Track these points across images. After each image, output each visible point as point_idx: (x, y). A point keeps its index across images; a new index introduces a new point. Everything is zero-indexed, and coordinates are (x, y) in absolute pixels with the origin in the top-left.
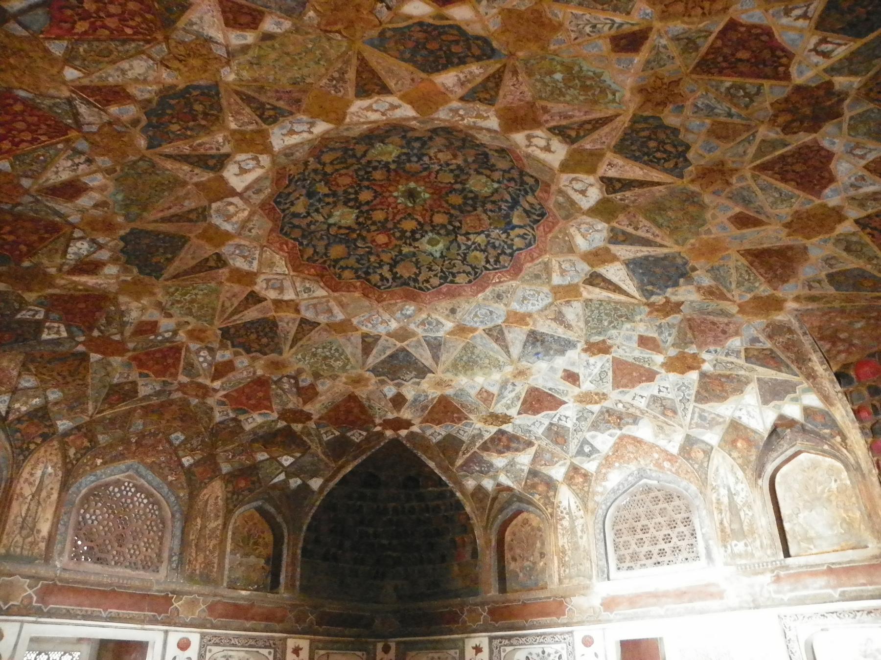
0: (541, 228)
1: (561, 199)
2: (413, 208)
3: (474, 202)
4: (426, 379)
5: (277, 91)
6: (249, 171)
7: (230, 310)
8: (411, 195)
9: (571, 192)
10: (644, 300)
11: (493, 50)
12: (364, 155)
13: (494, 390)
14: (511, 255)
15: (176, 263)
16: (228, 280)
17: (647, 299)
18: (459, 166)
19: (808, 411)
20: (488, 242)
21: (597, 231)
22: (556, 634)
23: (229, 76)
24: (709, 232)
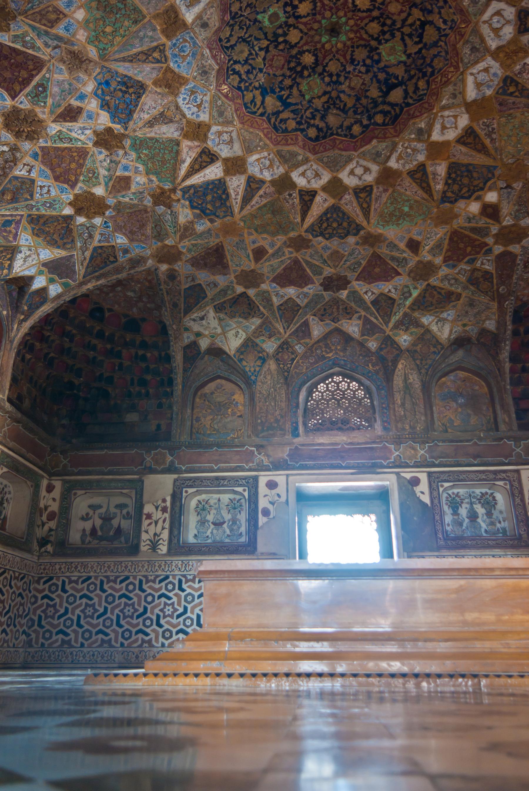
0: (265, 126)
1: (300, 158)
2: (319, 22)
5: (518, 108)
6: (493, 15)
8: (334, 31)
9: (305, 167)
10: (180, 187)
11: (445, 202)
12: (403, 39)
13: (60, 30)
14: (239, 88)
17: (181, 190)
18: (341, 84)
19: (44, 290)
20: (253, 68)
21: (261, 170)
24: (250, 234)
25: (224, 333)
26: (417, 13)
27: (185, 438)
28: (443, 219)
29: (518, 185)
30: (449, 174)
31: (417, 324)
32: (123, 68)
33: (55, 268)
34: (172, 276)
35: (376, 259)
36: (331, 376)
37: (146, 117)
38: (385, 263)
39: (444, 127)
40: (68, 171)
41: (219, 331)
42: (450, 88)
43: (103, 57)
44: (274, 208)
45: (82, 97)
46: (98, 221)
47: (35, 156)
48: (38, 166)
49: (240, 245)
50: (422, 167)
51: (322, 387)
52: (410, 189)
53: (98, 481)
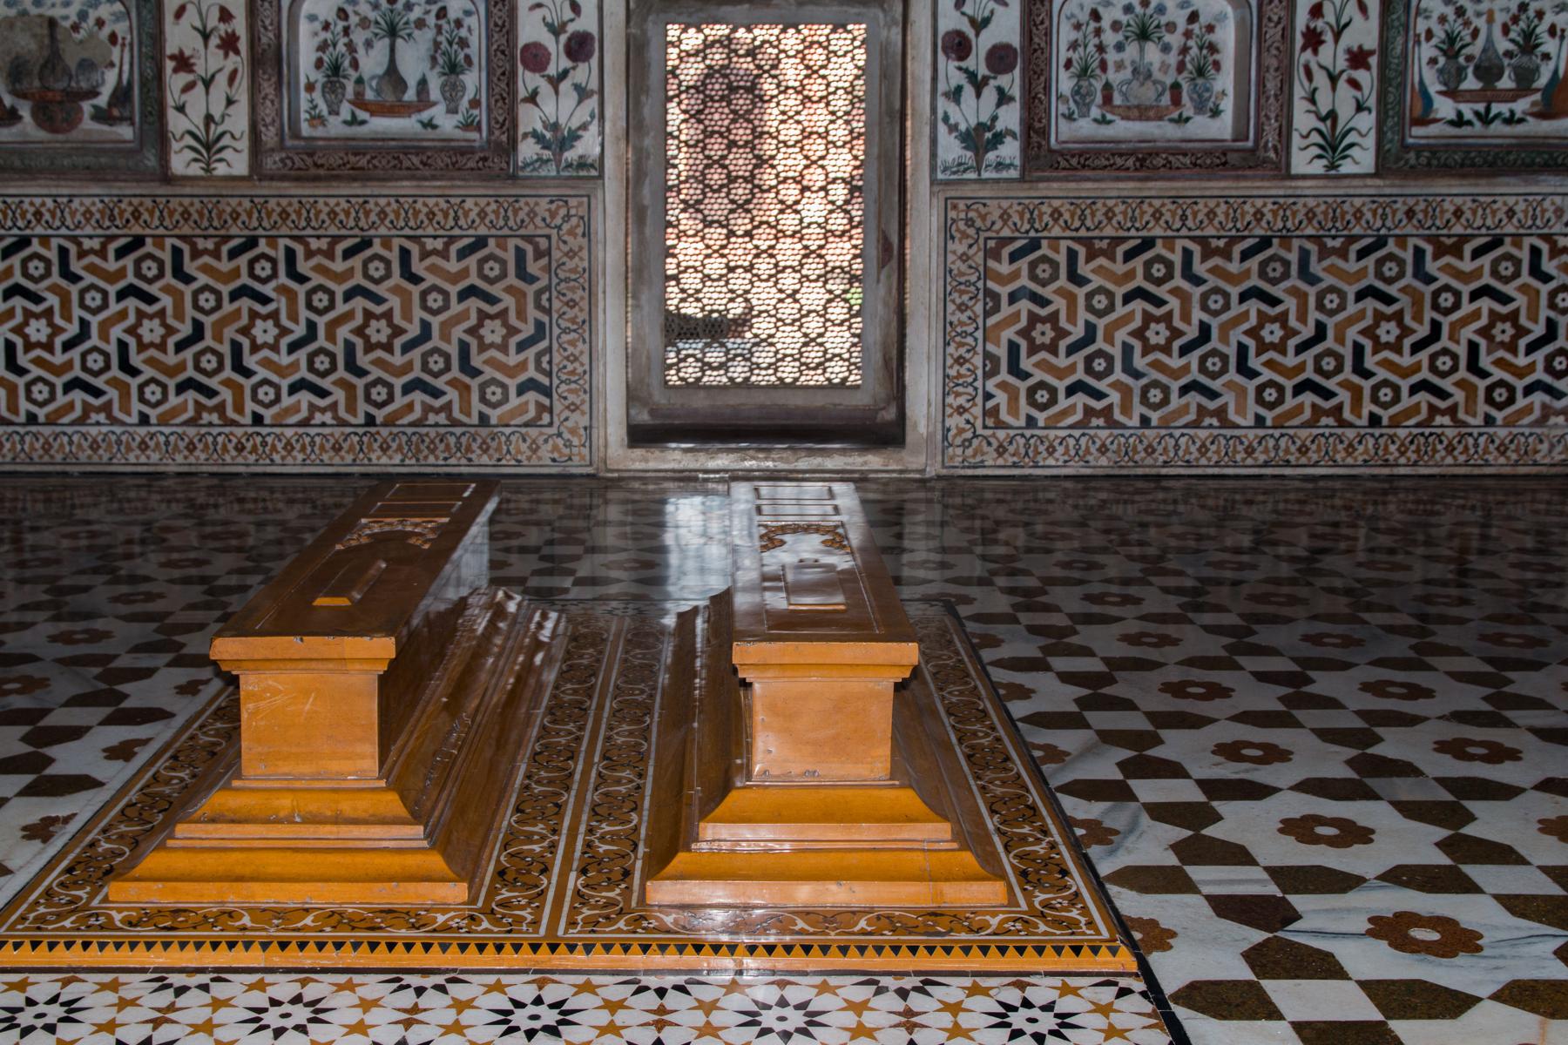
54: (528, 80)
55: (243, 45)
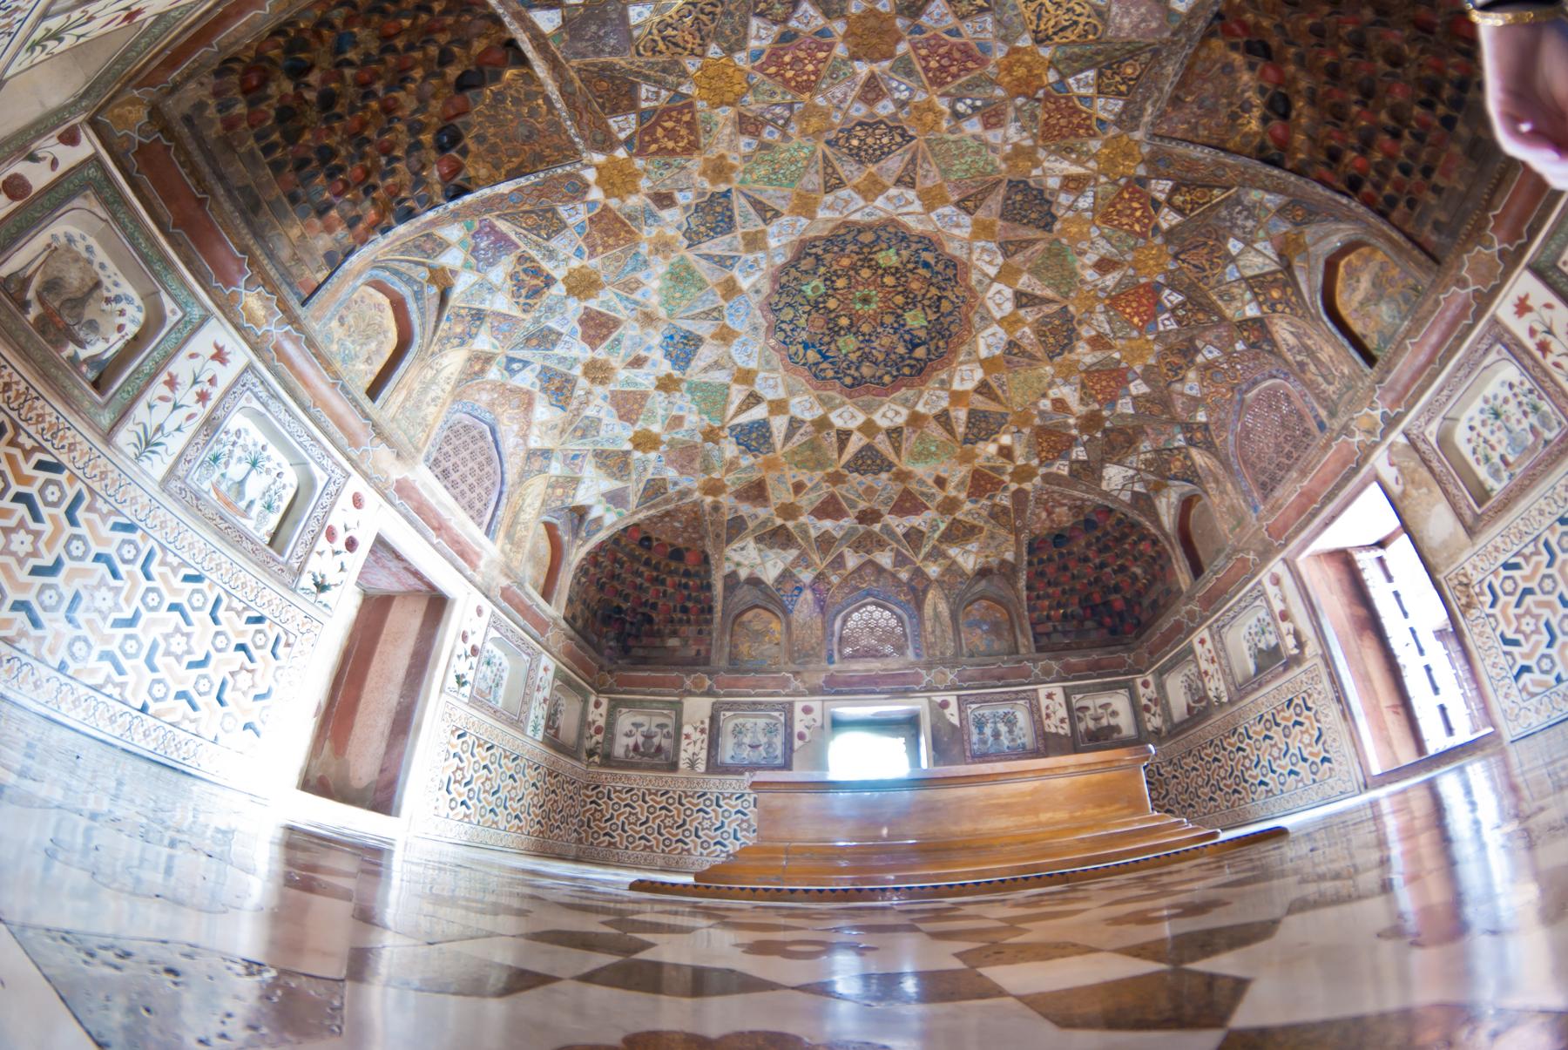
3: (835, 331)
4: (681, 238)
7: (919, 161)
8: (866, 300)
13: (637, 296)
15: (1000, 198)
16: (941, 186)
22: (330, 456)
23: (1049, 369)
25: (763, 563)
26: (934, 291)
27: (723, 663)
28: (966, 458)
29: (1026, 430)
30: (969, 418)
31: (944, 556)
32: (687, 325)
33: (615, 499)
34: (716, 508)
35: (907, 495)
36: (864, 605)
37: (702, 364)
38: (915, 498)
39: (962, 380)
40: (630, 411)
41: (758, 561)
42: (965, 348)
43: (670, 316)
44: (813, 445)
45: (649, 349)
46: (653, 455)
47: (605, 398)
48: (607, 407)
49: (780, 480)
50: (945, 412)
51: (855, 616)
52: (936, 431)
53: (641, 701)
54: (322, 543)
55: (210, 405)
